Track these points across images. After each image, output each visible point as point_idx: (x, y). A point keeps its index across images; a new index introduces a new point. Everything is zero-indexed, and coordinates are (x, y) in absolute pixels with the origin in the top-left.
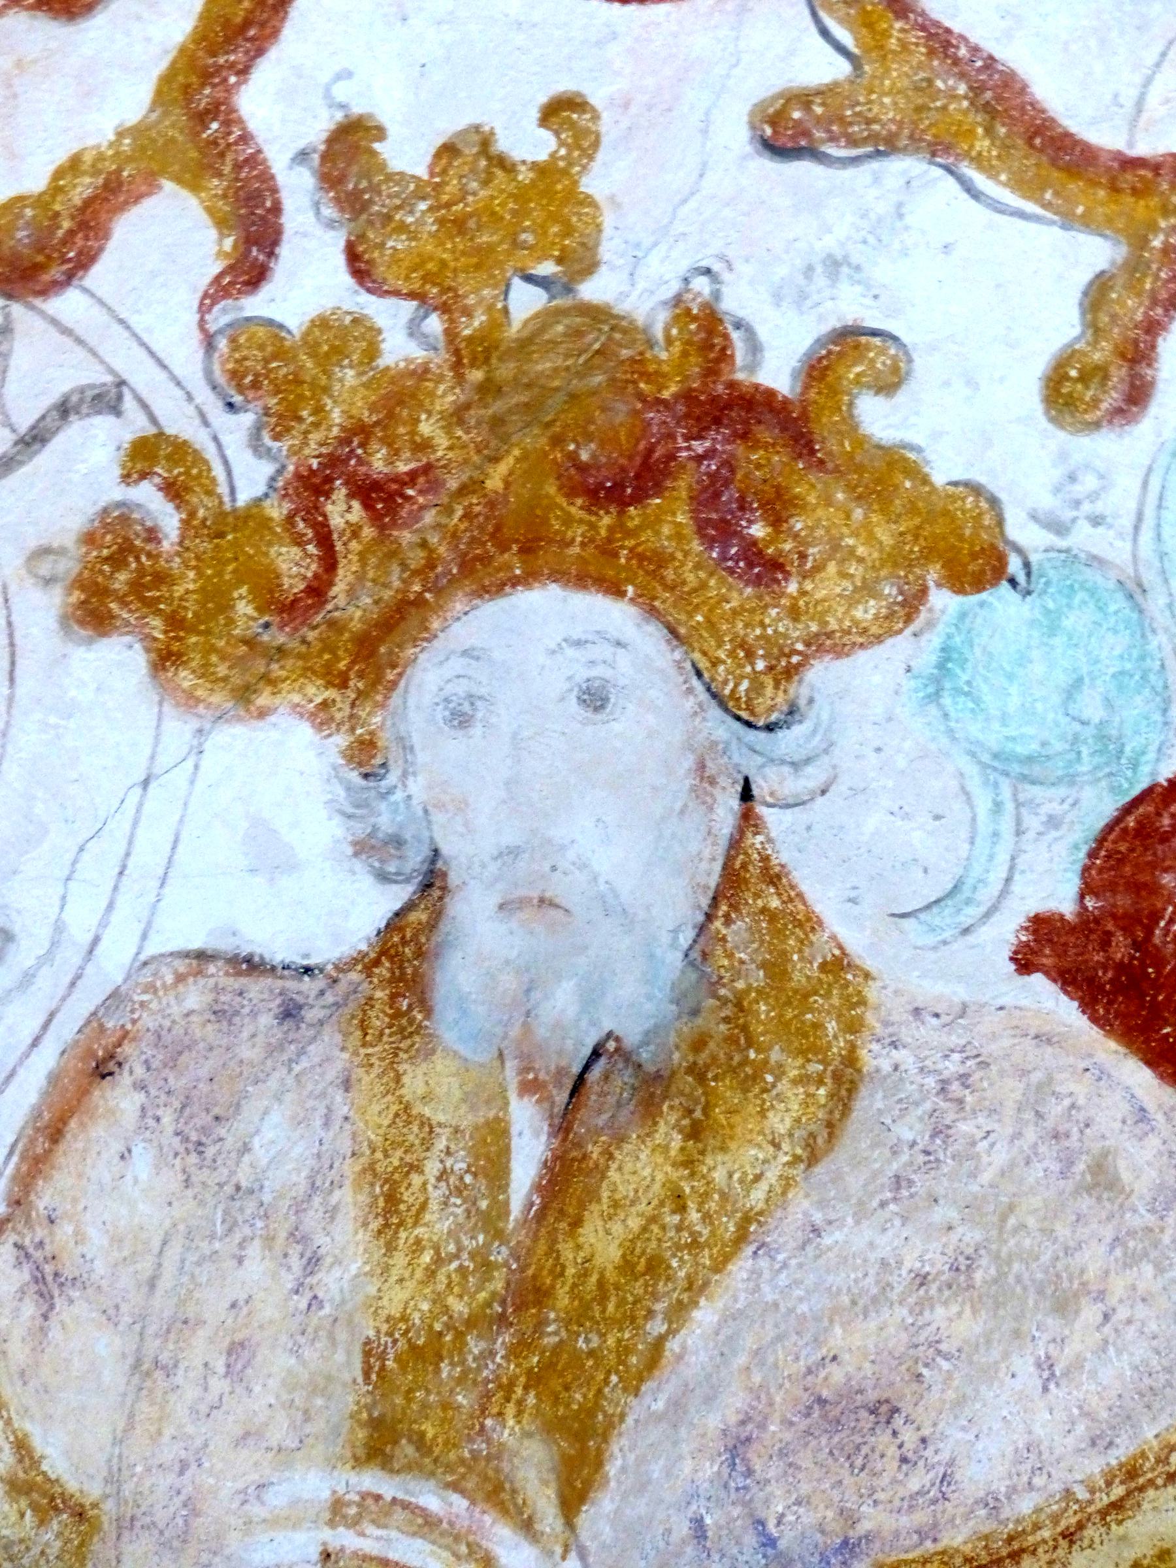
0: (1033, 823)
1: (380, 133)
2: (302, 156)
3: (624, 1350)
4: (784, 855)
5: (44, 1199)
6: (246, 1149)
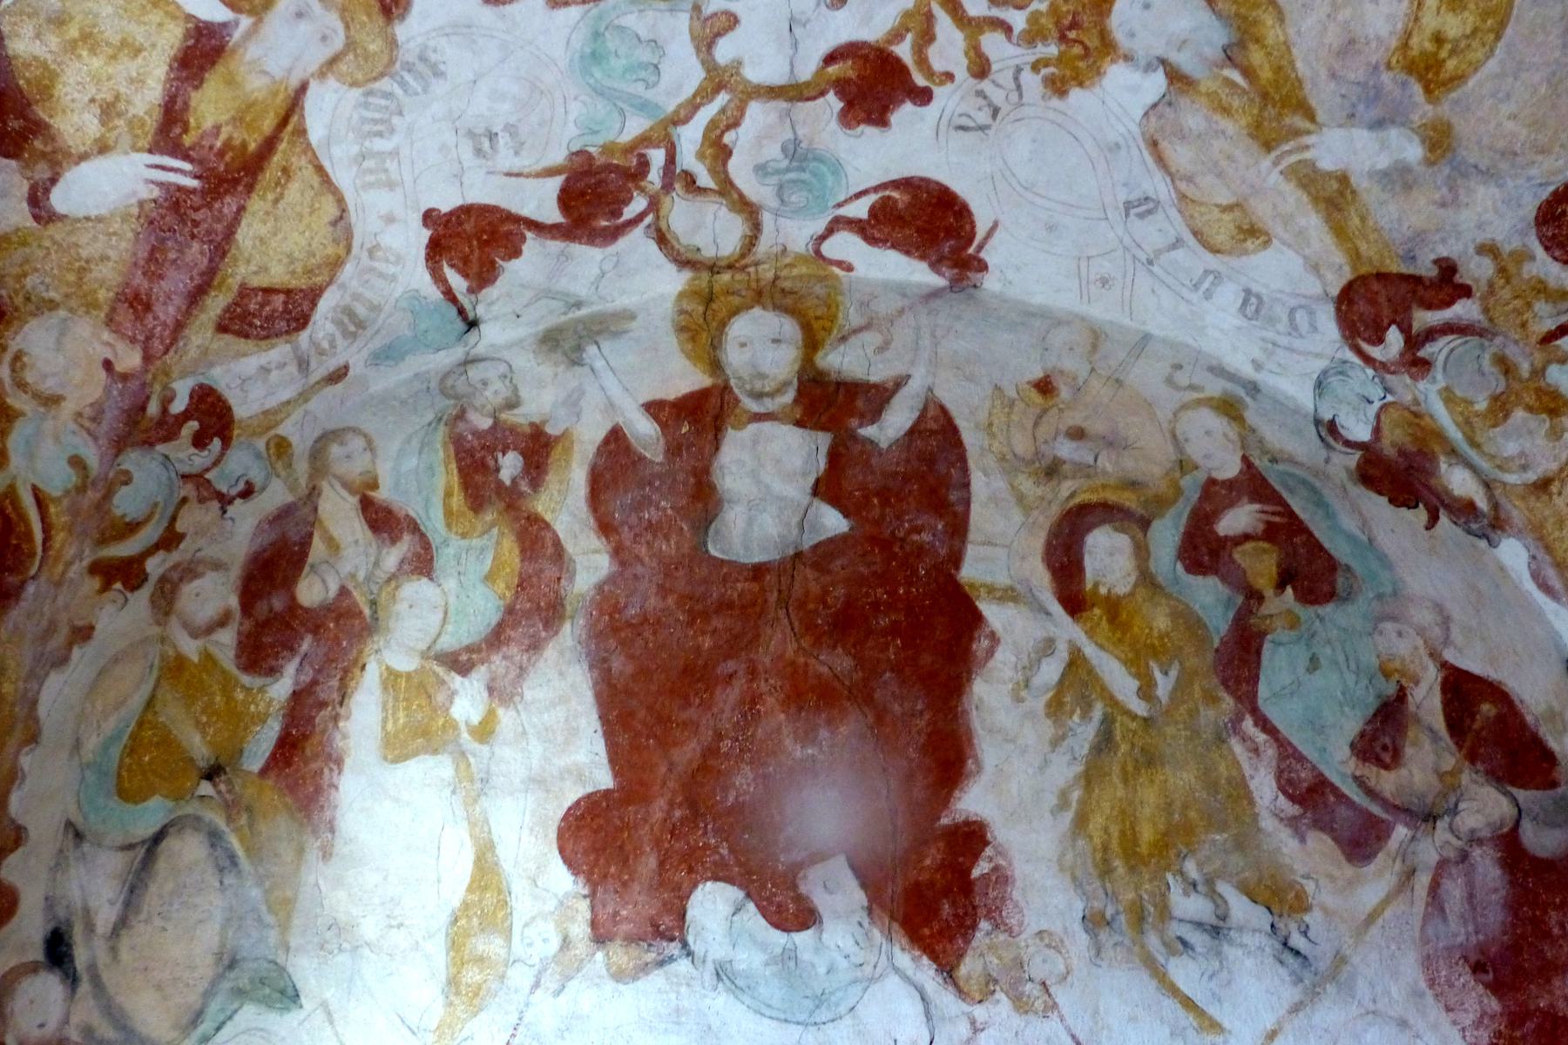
3: (1293, 84)
5: (1173, 170)
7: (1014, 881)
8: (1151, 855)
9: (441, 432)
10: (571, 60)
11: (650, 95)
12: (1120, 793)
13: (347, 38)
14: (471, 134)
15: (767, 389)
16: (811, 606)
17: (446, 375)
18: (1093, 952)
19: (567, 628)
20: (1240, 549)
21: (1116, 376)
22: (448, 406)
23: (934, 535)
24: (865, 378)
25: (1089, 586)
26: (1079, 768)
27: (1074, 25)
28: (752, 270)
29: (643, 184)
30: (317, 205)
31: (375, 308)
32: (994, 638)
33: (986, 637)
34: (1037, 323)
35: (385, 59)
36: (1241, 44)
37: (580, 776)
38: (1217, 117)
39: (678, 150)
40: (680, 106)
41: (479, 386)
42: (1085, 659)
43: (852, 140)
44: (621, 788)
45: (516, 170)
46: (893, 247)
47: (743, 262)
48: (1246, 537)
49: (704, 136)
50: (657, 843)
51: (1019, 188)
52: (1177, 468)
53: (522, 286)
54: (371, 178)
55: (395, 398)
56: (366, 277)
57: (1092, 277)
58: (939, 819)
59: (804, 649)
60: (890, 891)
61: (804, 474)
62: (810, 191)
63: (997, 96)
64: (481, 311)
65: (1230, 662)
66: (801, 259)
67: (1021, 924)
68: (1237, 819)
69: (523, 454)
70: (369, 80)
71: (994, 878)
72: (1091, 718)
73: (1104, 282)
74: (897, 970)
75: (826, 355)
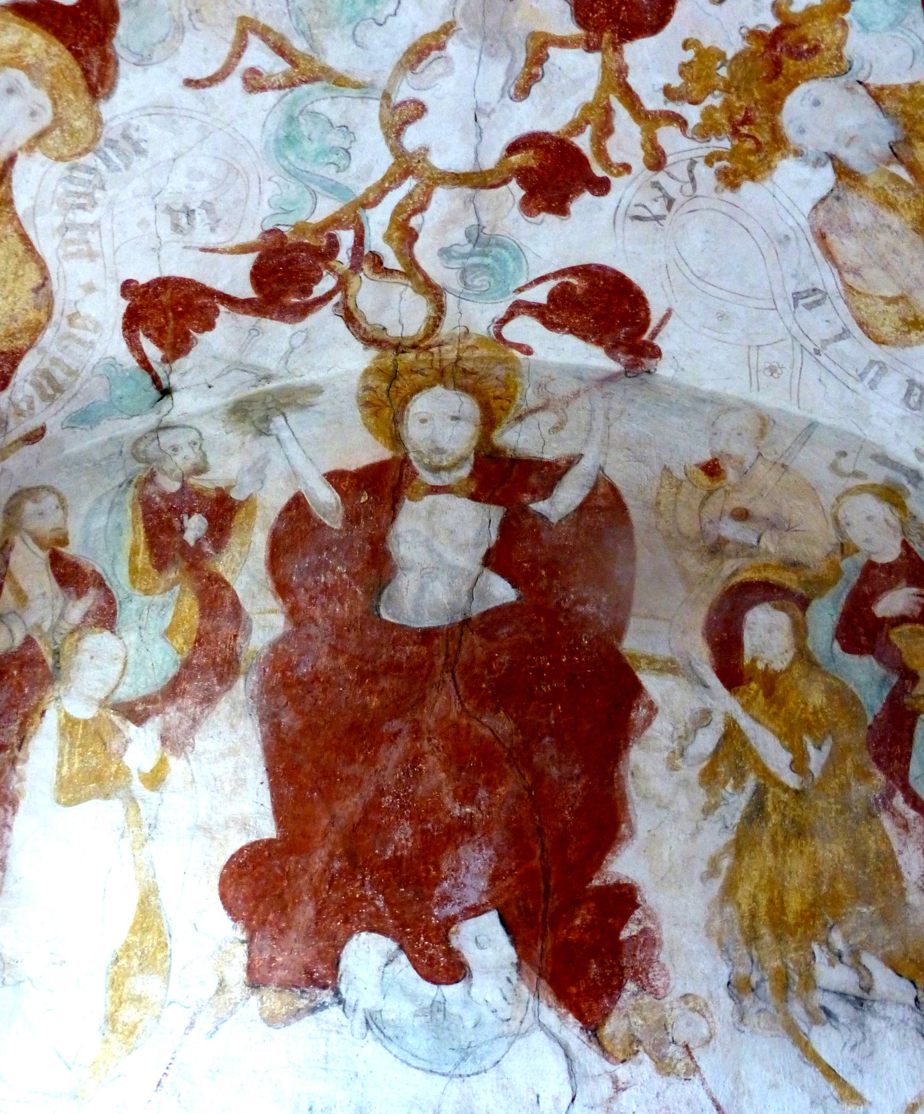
0: (912, 26)
1: (669, 85)
2: (665, 103)
4: (879, 84)
5: (840, 262)
6: (858, 224)
7: (660, 946)
8: (797, 925)
9: (131, 494)
10: (267, 142)
11: (341, 178)
12: (770, 861)
13: (55, 114)
14: (169, 210)
15: (445, 463)
16: (476, 670)
17: (140, 439)
18: (737, 1018)
19: (240, 682)
20: (898, 630)
21: (781, 461)
22: (139, 469)
23: (598, 607)
24: (539, 455)
25: (747, 661)
26: (730, 837)
27: (747, 121)
28: (435, 350)
29: (332, 263)
30: (21, 273)
31: (73, 373)
32: (652, 709)
33: (644, 707)
34: (708, 408)
35: (90, 135)
36: (907, 141)
37: (244, 826)
38: (883, 212)
39: (366, 232)
40: (369, 190)
41: (170, 451)
42: (740, 731)
43: (533, 227)
44: (283, 839)
45: (211, 246)
46: (571, 332)
47: (426, 343)
48: (902, 620)
49: (392, 219)
50: (316, 893)
51: (693, 278)
52: (838, 552)
53: (215, 357)
54: (72, 249)
55: (89, 461)
56: (65, 342)
57: (761, 365)
58: (591, 880)
59: (467, 711)
60: (539, 948)
61: (477, 545)
62: (492, 275)
63: (672, 188)
64: (174, 380)
65: (883, 739)
66: (482, 340)
67: (666, 986)
68: (884, 893)
69: (206, 516)
70: (72, 156)
71: (642, 940)
72: (743, 789)
73: (772, 370)
74: (542, 1026)
75: (503, 432)
